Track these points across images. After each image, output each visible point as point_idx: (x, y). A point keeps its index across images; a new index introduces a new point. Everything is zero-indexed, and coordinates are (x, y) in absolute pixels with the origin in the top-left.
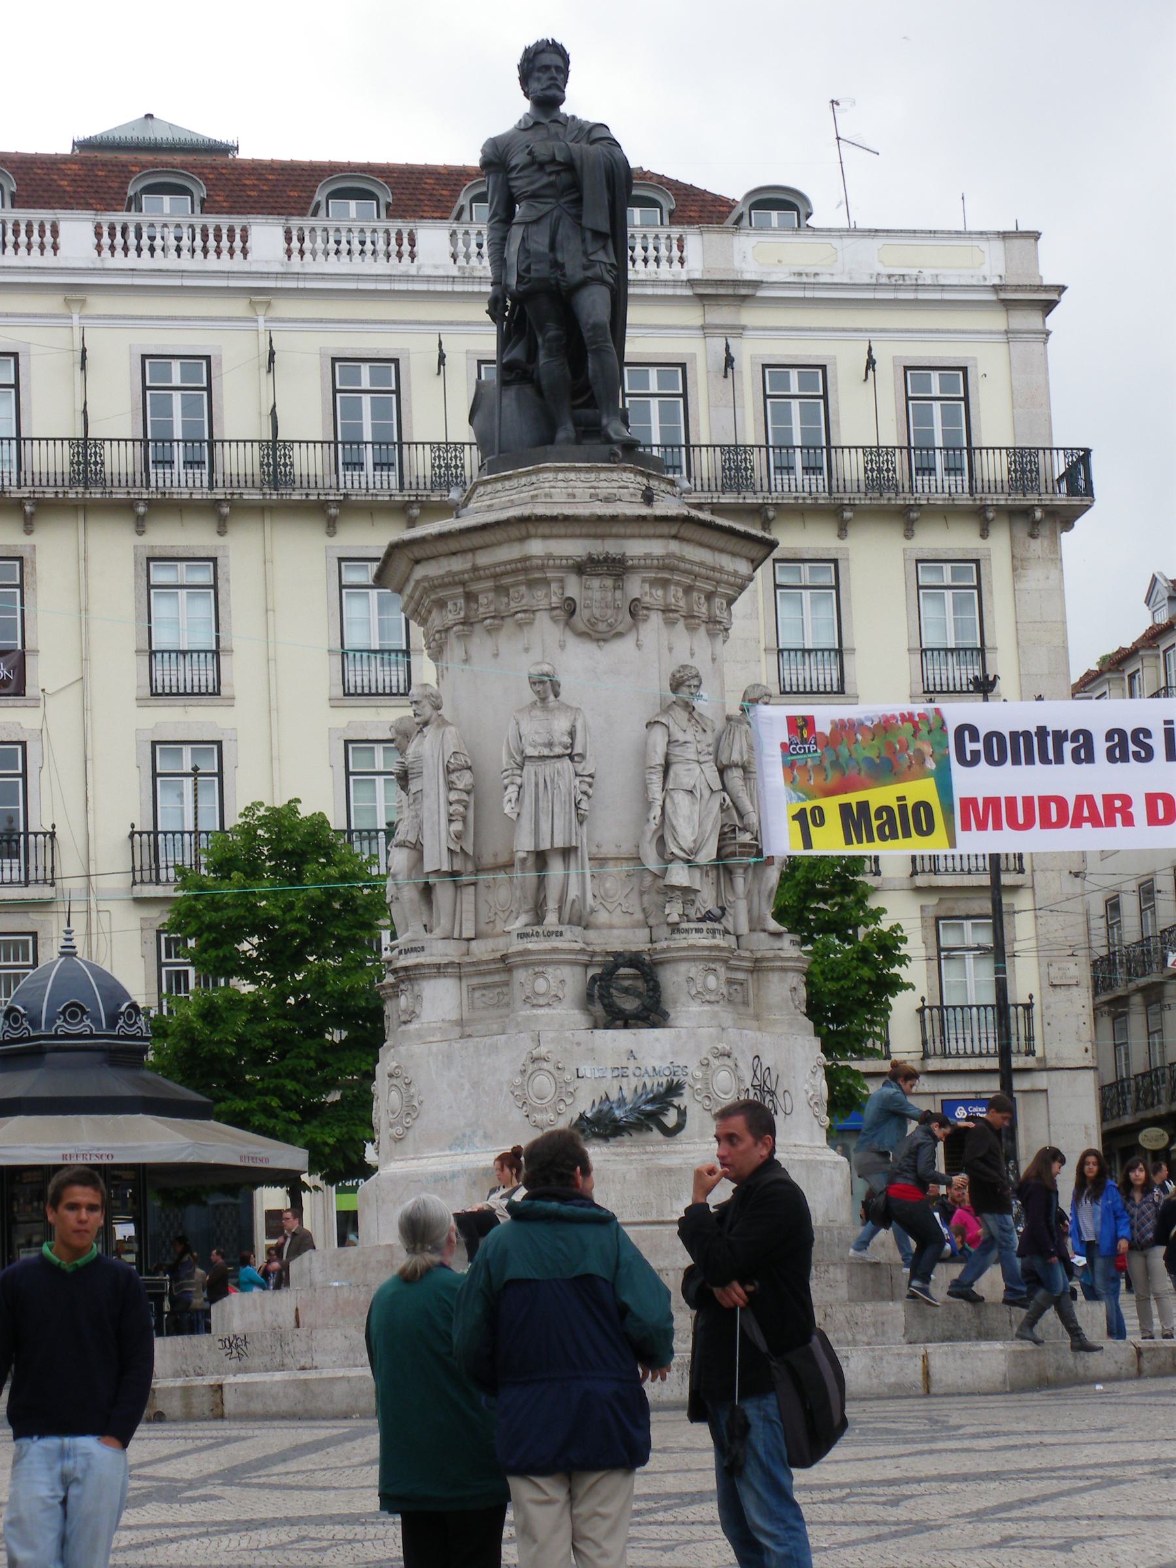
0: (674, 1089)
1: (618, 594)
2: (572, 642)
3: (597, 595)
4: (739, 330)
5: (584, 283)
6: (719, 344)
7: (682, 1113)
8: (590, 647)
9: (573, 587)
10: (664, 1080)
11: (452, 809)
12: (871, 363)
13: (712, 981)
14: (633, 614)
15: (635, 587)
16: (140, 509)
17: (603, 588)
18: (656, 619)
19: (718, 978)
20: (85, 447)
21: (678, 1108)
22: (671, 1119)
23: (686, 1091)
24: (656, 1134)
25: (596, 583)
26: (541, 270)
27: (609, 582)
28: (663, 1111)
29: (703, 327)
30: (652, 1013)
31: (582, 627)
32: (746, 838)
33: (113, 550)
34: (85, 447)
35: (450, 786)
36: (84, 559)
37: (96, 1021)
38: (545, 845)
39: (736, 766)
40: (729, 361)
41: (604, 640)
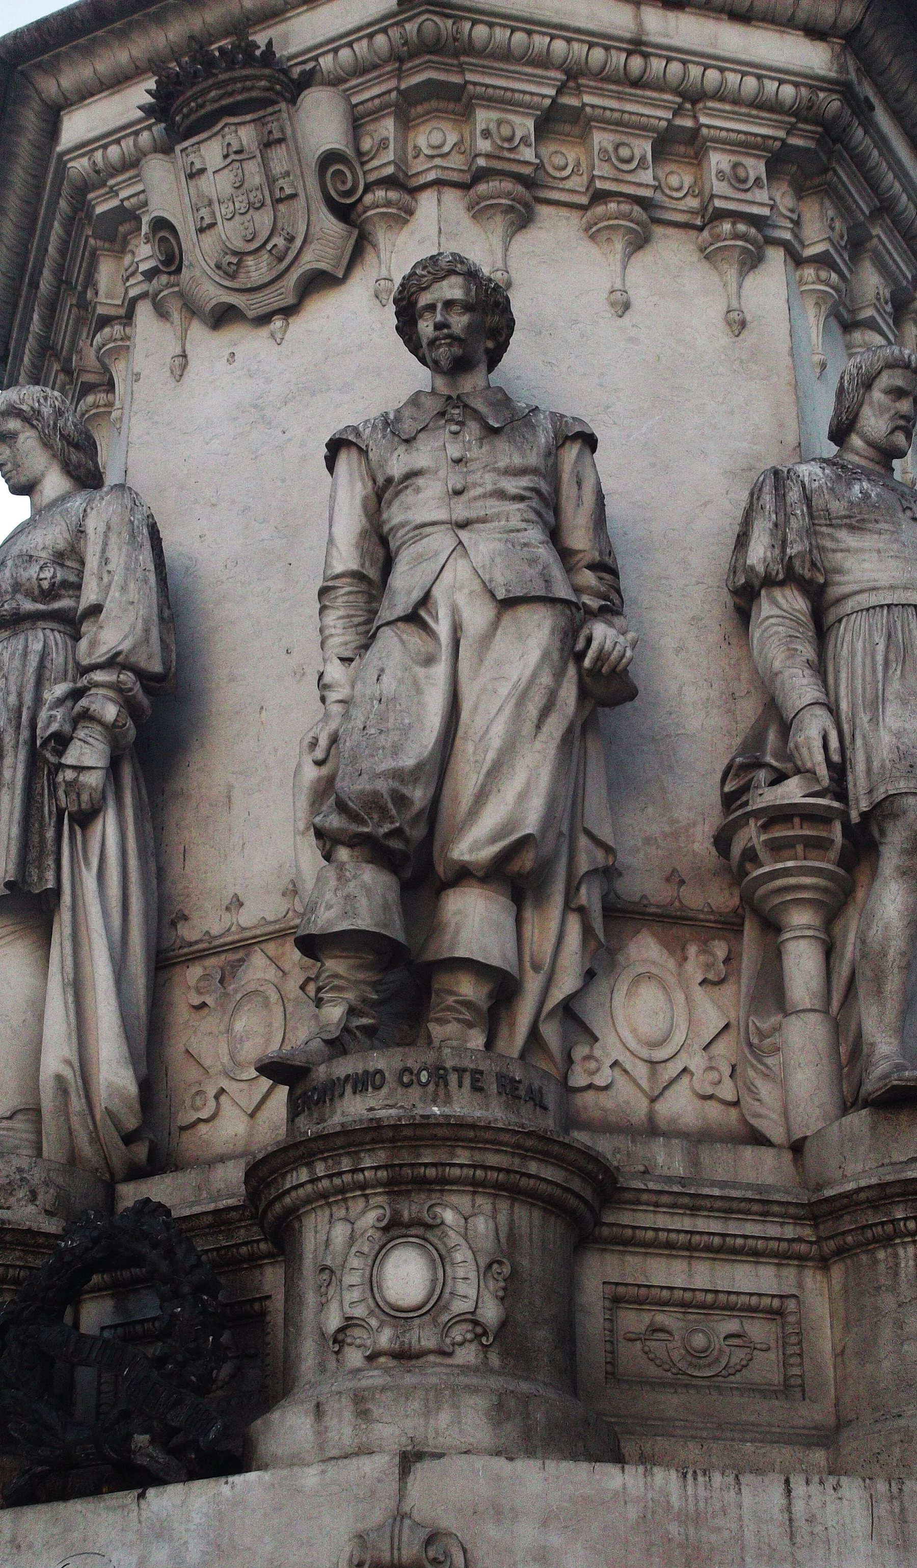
1: (279, 159)
2: (206, 345)
8: (251, 344)
13: (406, 1276)
14: (344, 212)
15: (320, 122)
19: (440, 1260)
31: (212, 293)
32: (792, 791)
39: (769, 582)
41: (288, 312)
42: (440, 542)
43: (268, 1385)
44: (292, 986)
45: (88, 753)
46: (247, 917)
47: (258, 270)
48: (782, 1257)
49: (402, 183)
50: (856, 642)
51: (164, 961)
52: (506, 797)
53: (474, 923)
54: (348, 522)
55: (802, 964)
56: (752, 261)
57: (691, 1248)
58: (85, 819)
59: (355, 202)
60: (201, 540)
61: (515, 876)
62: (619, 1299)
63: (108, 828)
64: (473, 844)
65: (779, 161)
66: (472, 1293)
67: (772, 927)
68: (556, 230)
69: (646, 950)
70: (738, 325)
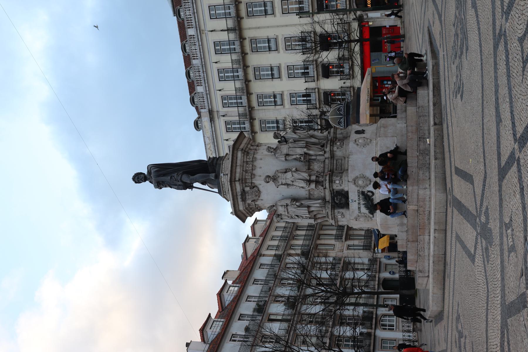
0: (363, 193)
2: (261, 198)
3: (250, 197)
5: (182, 181)
7: (369, 191)
9: (249, 201)
10: (361, 195)
13: (337, 182)
14: (254, 187)
15: (247, 189)
16: (239, 18)
17: (248, 195)
20: (228, 30)
22: (369, 194)
23: (364, 190)
24: (374, 197)
25: (247, 197)
30: (345, 195)
32: (302, 158)
33: (247, 23)
34: (228, 30)
36: (250, 29)
37: (341, 118)
42: (287, 180)
43: (343, 190)
45: (298, 204)
47: (257, 194)
48: (333, 160)
49: (252, 183)
50: (291, 153)
51: (310, 199)
52: (305, 175)
53: (313, 178)
54: (283, 186)
55: (313, 157)
56: (256, 158)
57: (333, 166)
58: (302, 204)
59: (253, 186)
60: (279, 197)
61: (310, 176)
62: (336, 170)
63: (303, 202)
64: (308, 178)
65: (247, 155)
66: (339, 178)
67: (310, 159)
68: (254, 172)
69: (311, 167)
70: (261, 159)
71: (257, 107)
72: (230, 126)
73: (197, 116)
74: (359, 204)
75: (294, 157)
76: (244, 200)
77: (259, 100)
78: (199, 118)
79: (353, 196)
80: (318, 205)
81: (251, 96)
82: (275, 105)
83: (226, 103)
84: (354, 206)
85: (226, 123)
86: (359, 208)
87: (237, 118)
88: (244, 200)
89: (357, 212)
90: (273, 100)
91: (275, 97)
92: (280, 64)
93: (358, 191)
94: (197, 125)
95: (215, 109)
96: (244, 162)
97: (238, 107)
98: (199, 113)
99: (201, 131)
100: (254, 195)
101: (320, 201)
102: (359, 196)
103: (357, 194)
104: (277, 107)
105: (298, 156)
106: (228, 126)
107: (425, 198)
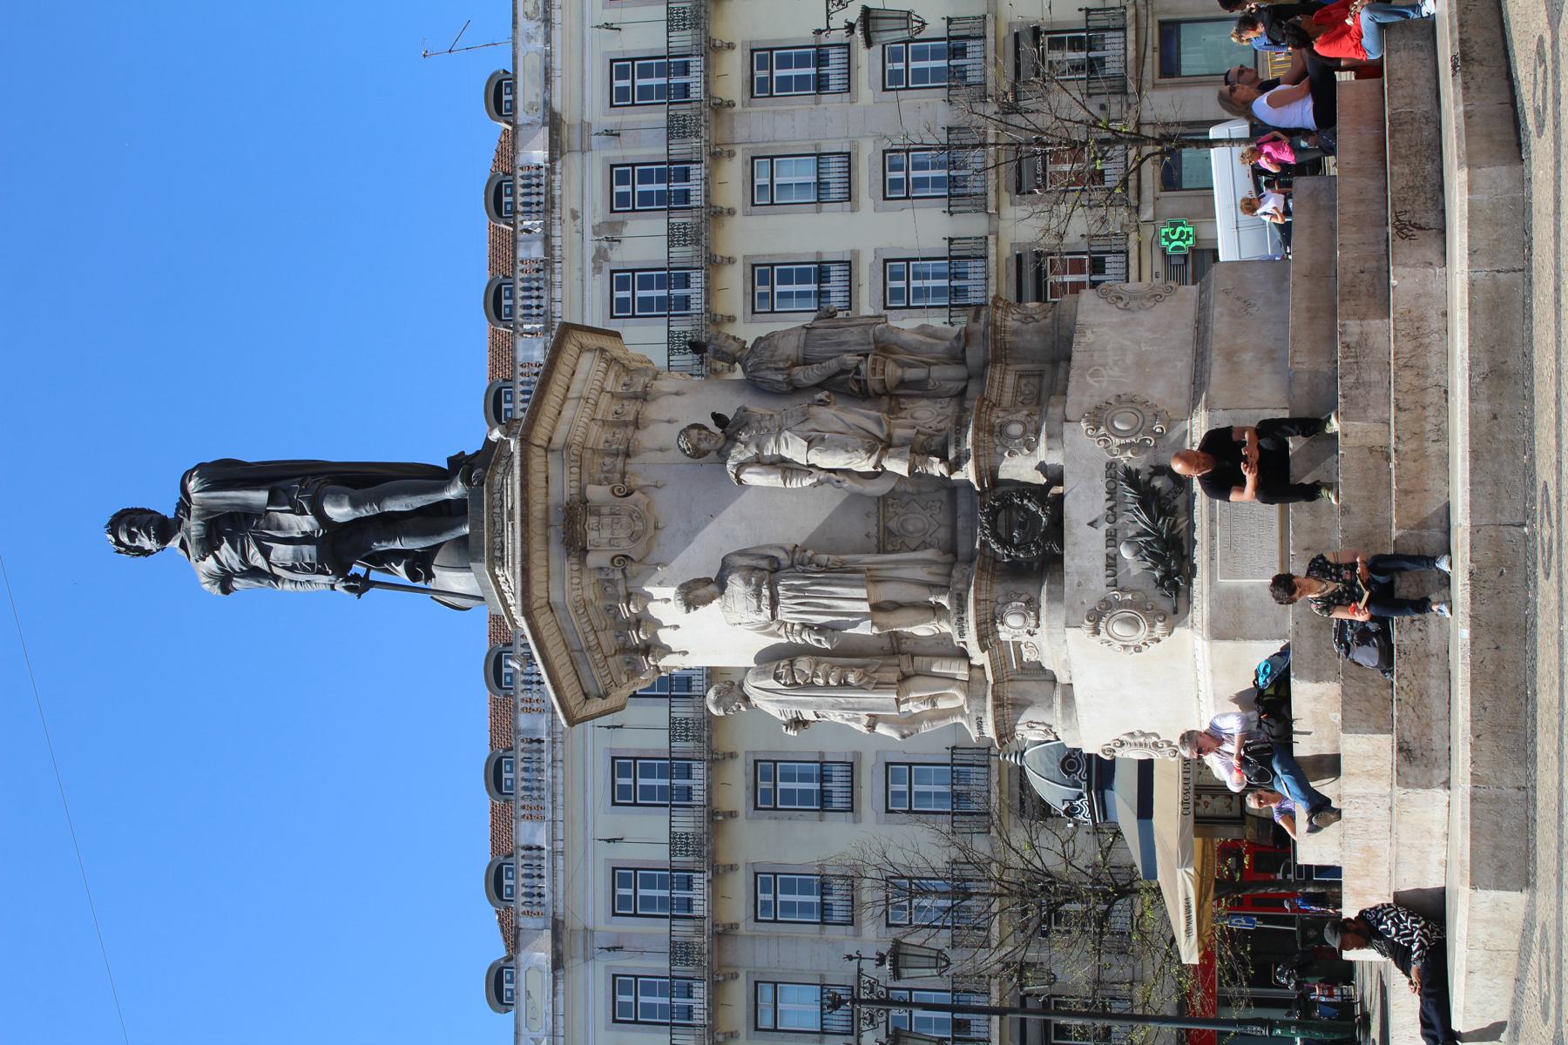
0: (1131, 477)
1: (605, 510)
3: (606, 534)
4: (585, 127)
6: (595, 139)
11: (832, 682)
12: (608, 26)
15: (597, 493)
18: (634, 464)
19: (1011, 422)
21: (1152, 475)
25: (592, 536)
26: (309, 551)
27: (592, 520)
28: (1155, 492)
29: (583, 151)
35: (810, 686)
38: (865, 607)
40: (609, 133)
44: (900, 511)
46: (874, 531)
71: (746, 926)
72: (630, 999)
73: (499, 951)
74: (1112, 538)
75: (833, 365)
76: (576, 547)
77: (761, 896)
78: (509, 959)
79: (1084, 503)
80: (921, 574)
81: (731, 877)
82: (823, 923)
83: (625, 901)
84: (1084, 548)
85: (618, 983)
86: (1112, 562)
87: (660, 965)
88: (576, 547)
89: (1098, 585)
90: (816, 899)
91: (824, 888)
92: (858, 755)
93: (1111, 466)
94: (499, 988)
95: (574, 923)
96: (602, 390)
97: (673, 917)
98: (514, 938)
99: (511, 1014)
100: (622, 534)
101: (928, 554)
102: (1112, 494)
103: (1101, 483)
104: (833, 932)
105: (851, 359)
106: (621, 998)
107: (1422, 318)
